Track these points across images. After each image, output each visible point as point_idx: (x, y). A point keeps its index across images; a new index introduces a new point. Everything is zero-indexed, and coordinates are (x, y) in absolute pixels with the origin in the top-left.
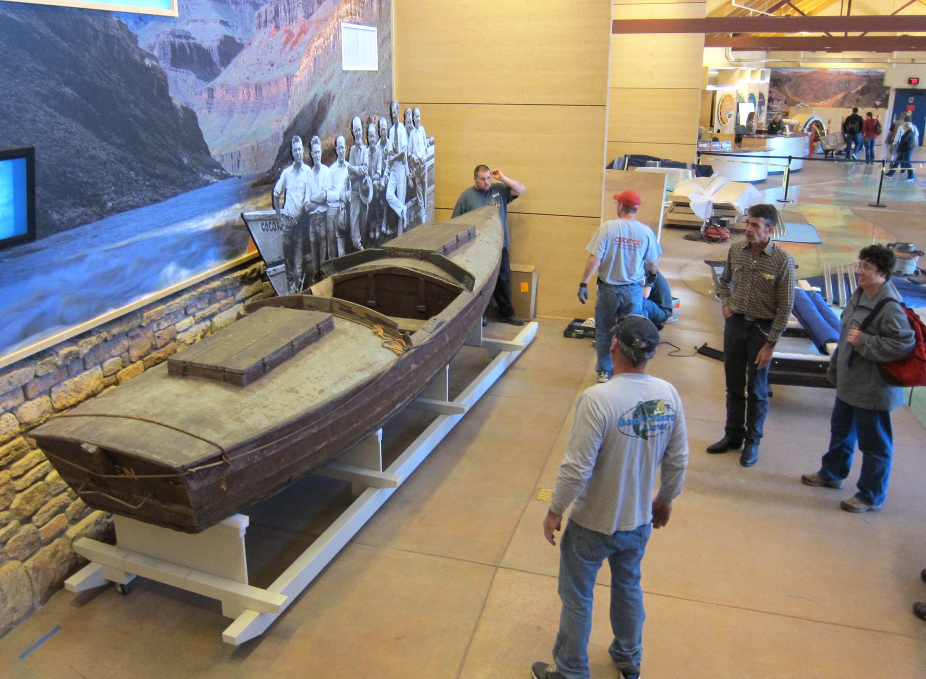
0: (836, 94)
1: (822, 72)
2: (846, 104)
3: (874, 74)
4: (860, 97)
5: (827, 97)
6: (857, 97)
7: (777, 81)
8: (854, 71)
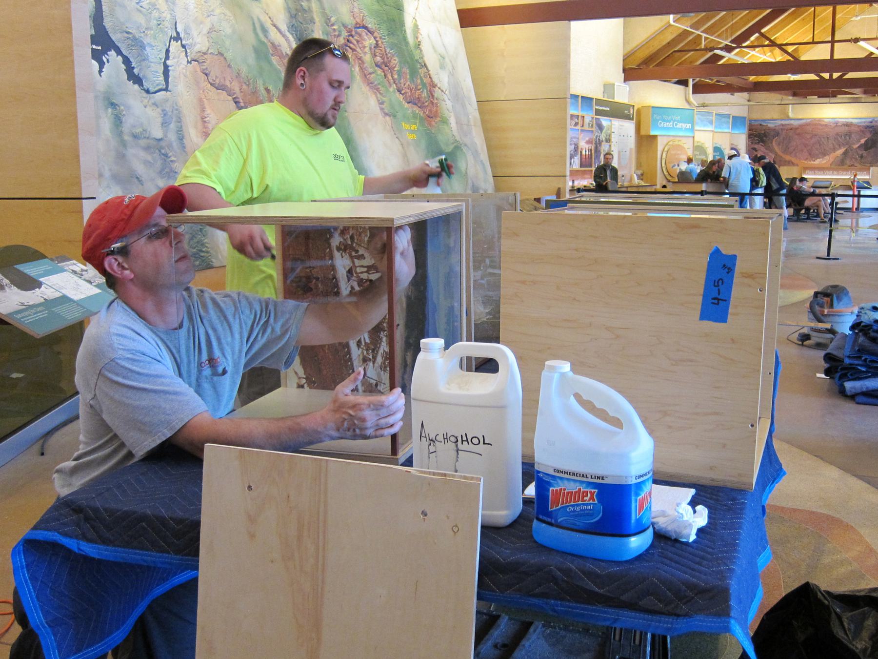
0: (834, 150)
1: (816, 124)
2: (848, 162)
4: (865, 153)
5: (824, 154)
6: (860, 152)
7: (759, 135)
8: (855, 121)
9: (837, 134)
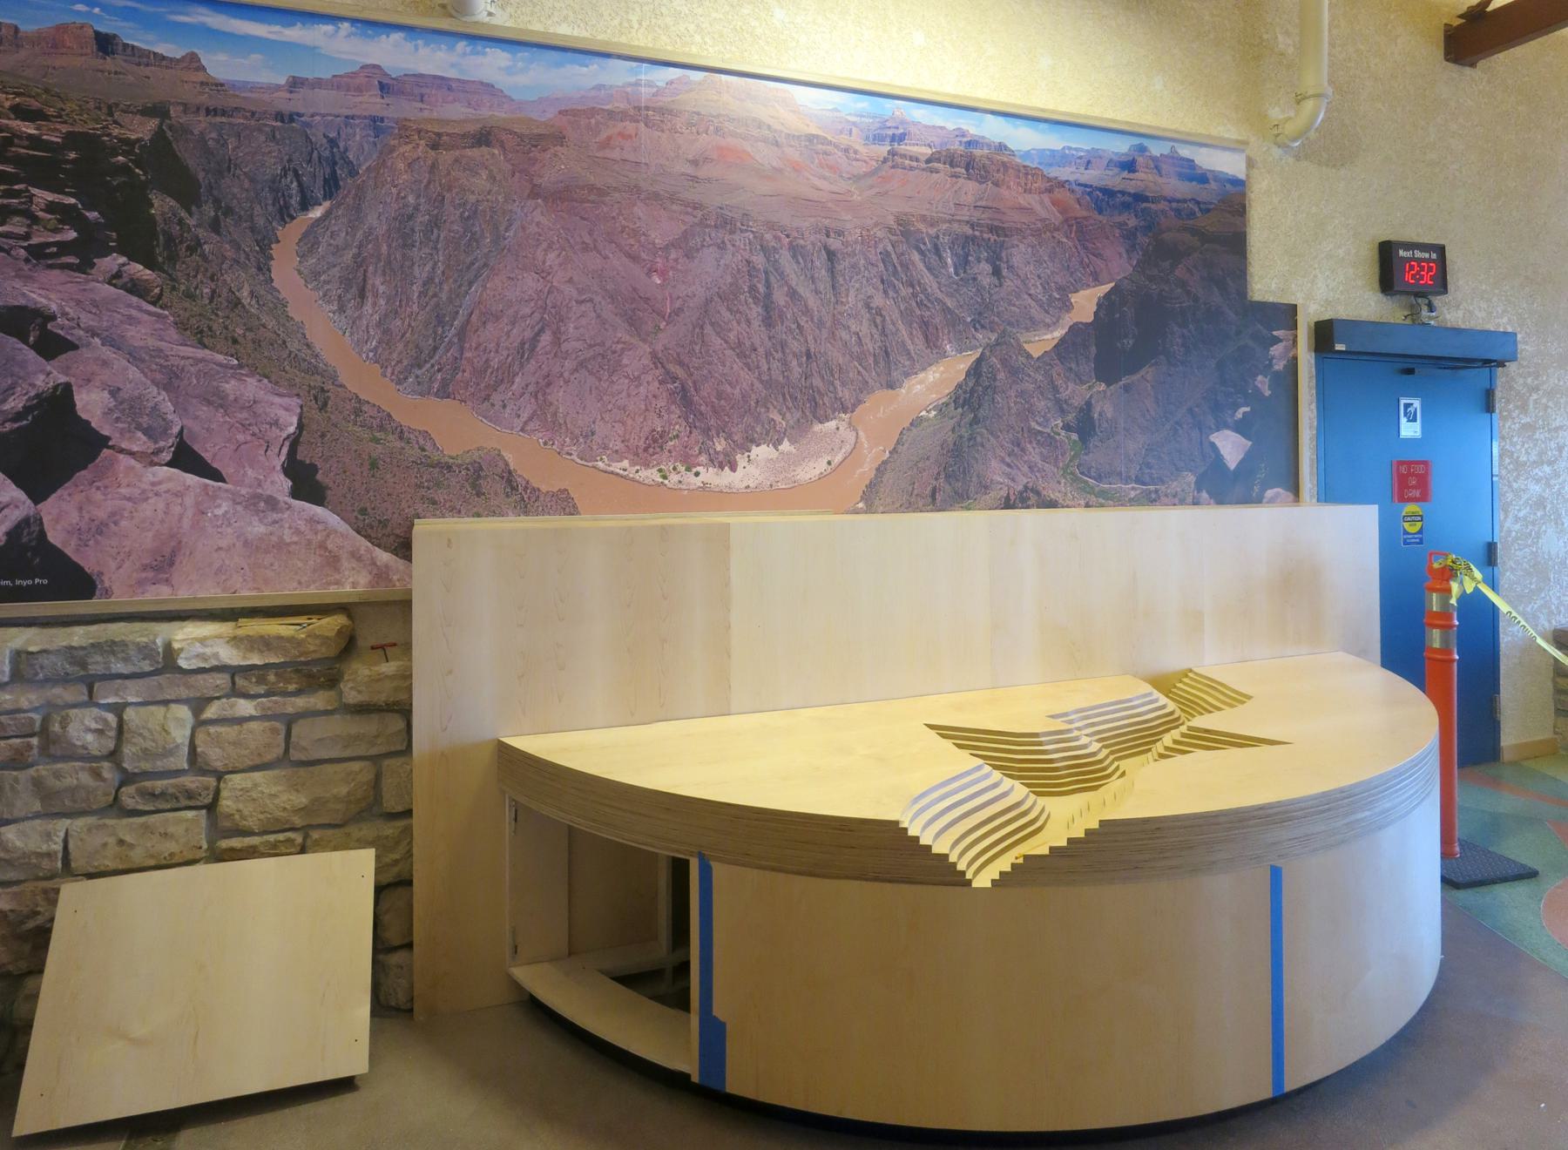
0: (889, 366)
3: (1175, 186)
4: (1105, 401)
5: (810, 399)
8: (1024, 140)
9: (904, 229)
